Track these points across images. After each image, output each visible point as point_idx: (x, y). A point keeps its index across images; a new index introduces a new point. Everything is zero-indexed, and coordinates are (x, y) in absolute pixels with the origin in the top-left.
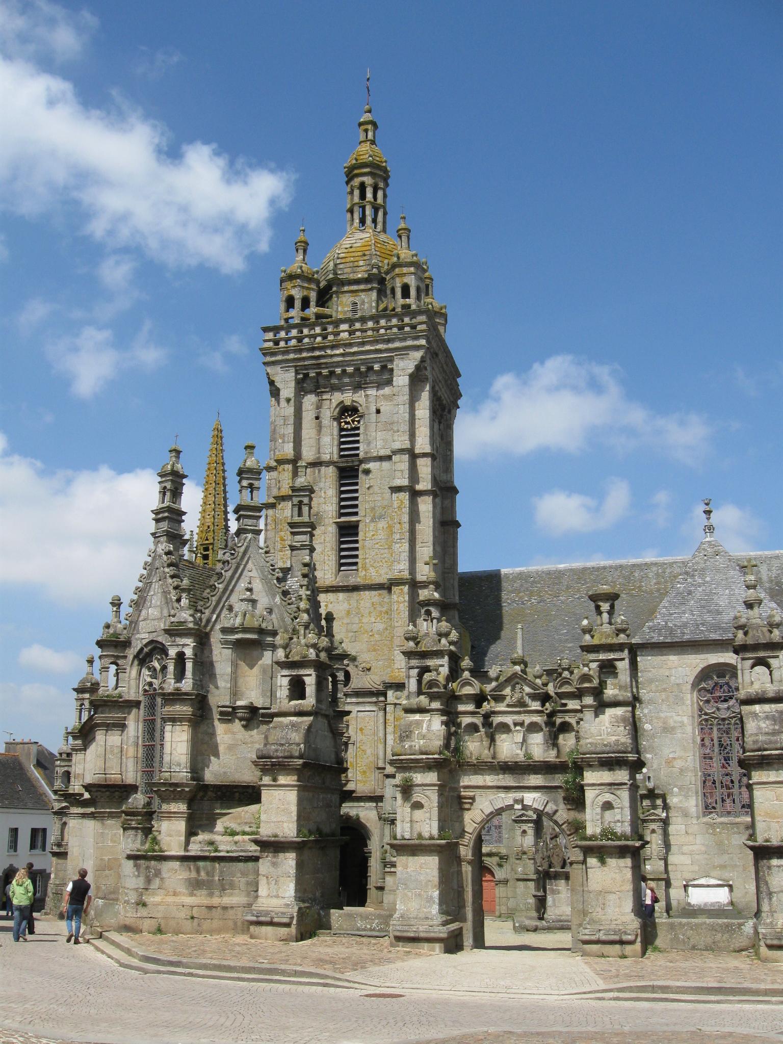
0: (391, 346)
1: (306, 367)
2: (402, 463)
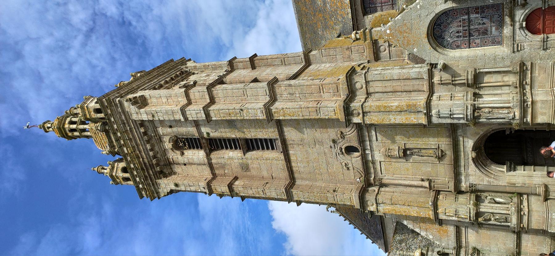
0: (125, 121)
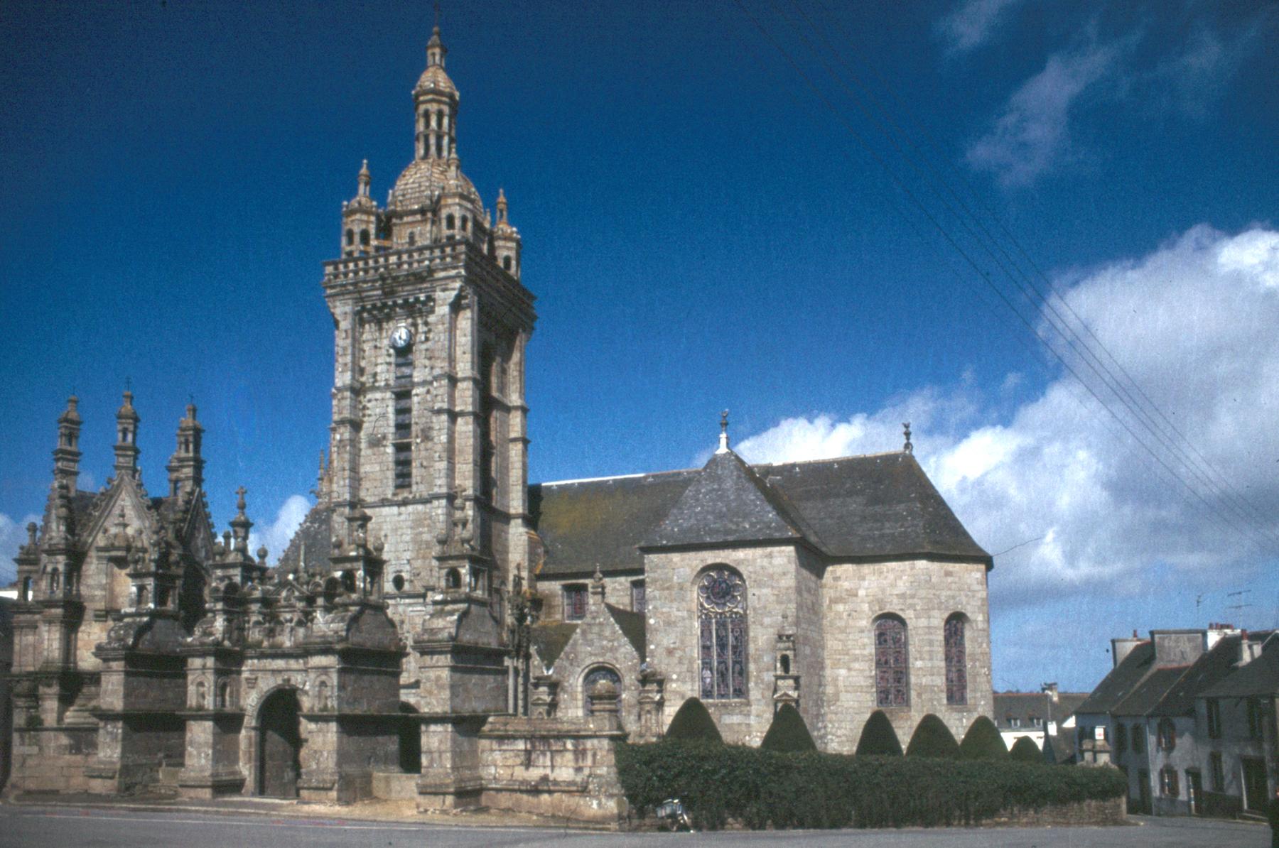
2: (441, 387)
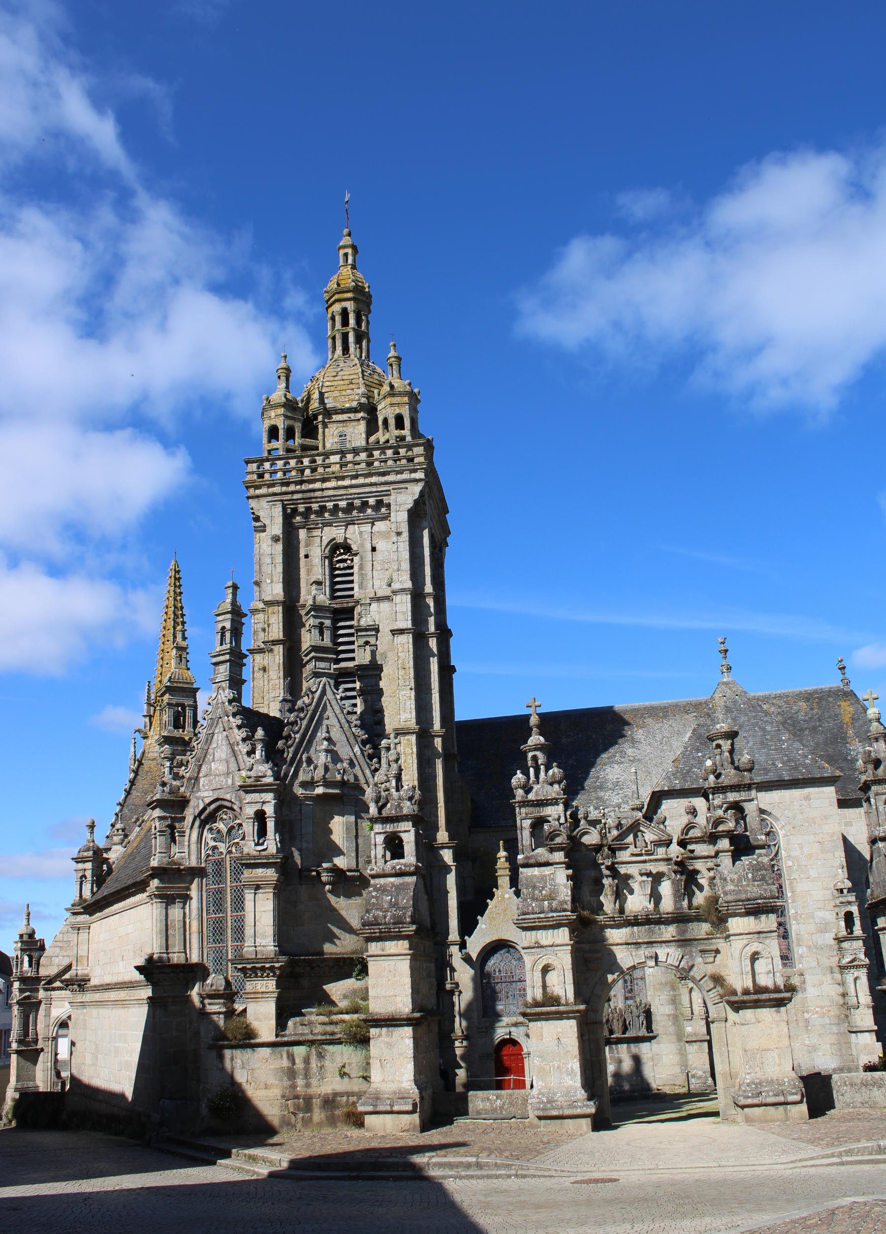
1: (295, 502)
